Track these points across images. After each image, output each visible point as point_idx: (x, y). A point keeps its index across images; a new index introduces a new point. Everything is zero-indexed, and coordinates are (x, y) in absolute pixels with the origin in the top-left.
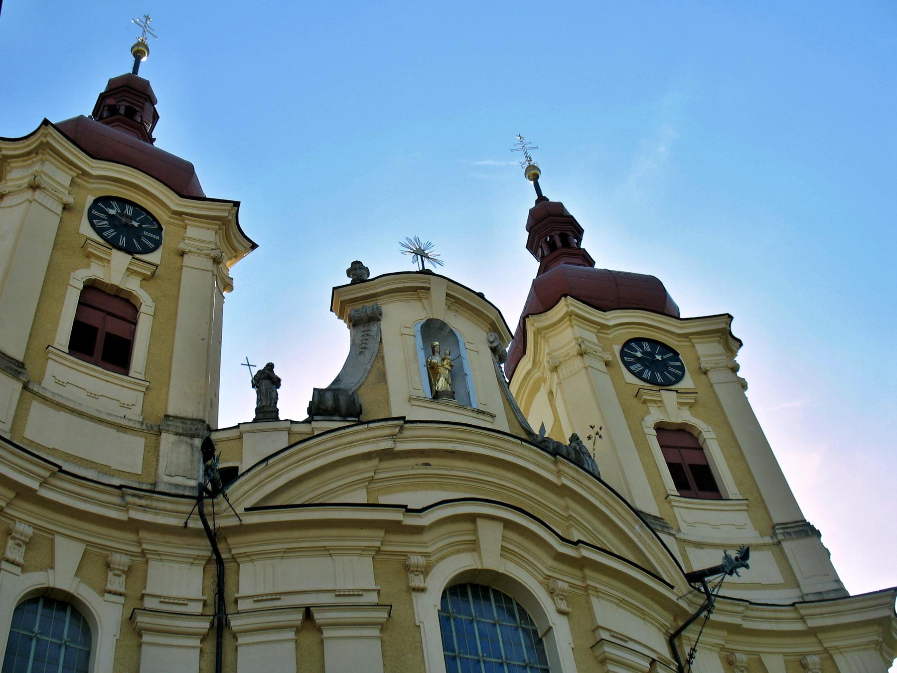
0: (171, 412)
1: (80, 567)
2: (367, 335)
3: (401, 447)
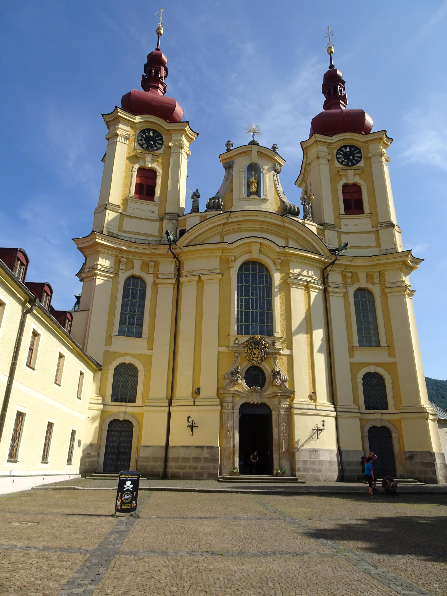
0: (167, 212)
3: (230, 220)
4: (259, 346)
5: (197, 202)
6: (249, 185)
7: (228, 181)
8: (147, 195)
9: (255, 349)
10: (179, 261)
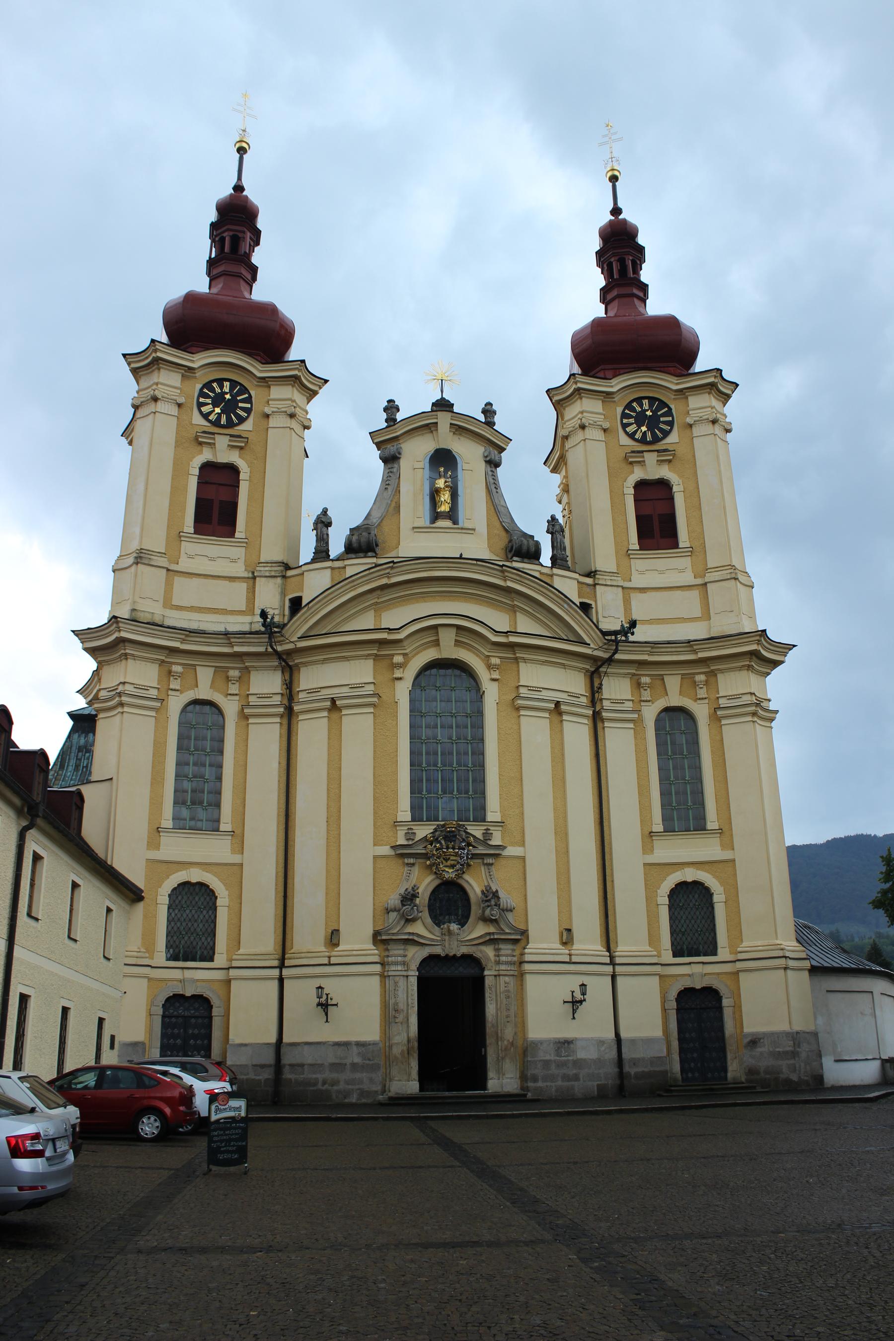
2: (391, 472)
4: (455, 843)
9: (447, 848)
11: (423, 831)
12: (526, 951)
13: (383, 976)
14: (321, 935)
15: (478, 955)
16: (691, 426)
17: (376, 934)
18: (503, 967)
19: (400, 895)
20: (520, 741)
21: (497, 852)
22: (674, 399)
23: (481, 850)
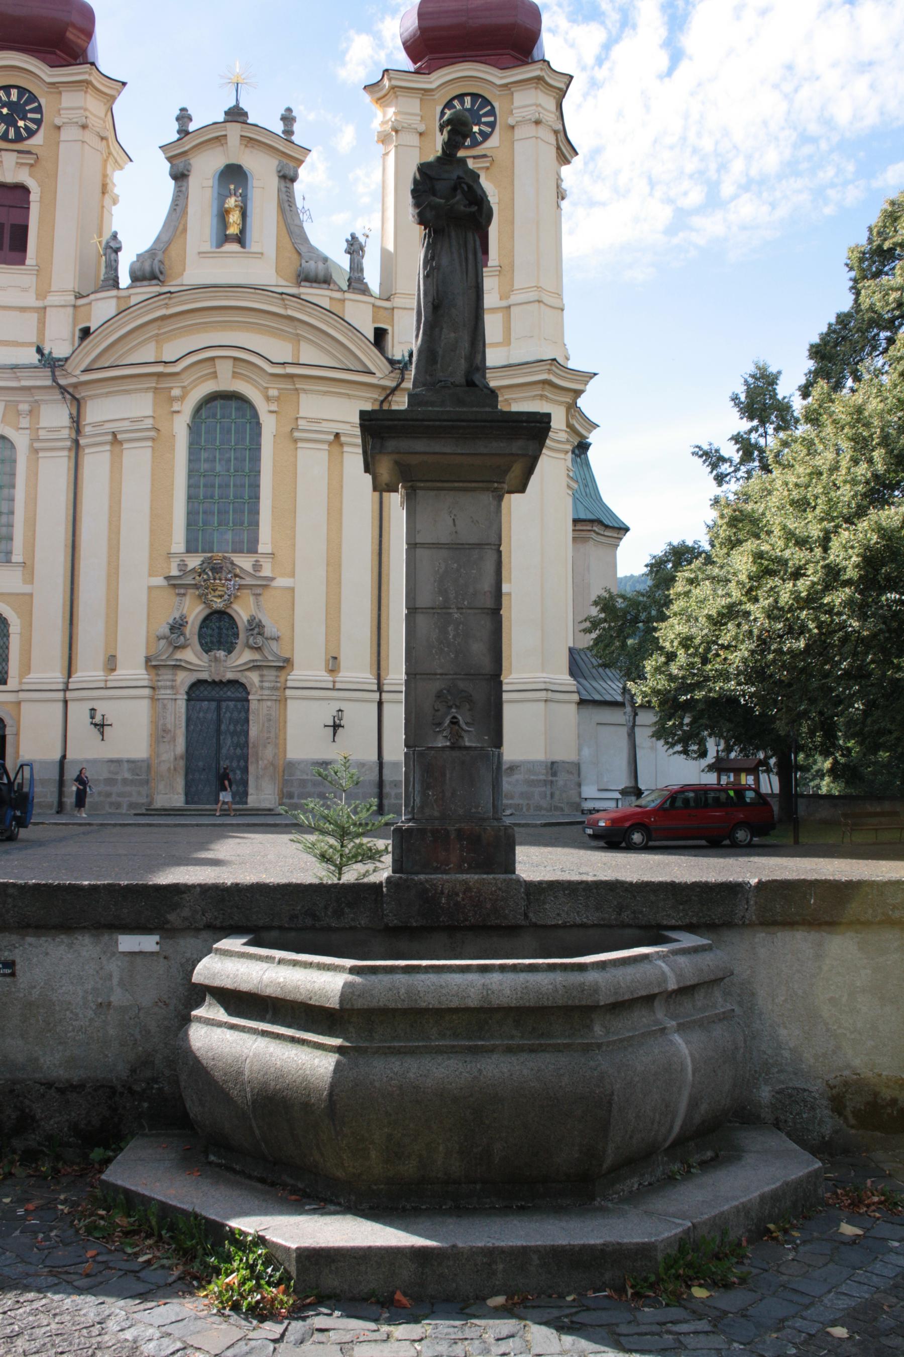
1: (4, 416)
5: (113, 263)
6: (223, 215)
7: (179, 209)
8: (13, 248)
9: (215, 579)
10: (78, 400)
11: (194, 562)
12: (289, 677)
13: (152, 698)
14: (101, 659)
15: (243, 680)
16: (513, 127)
17: (148, 660)
18: (266, 692)
19: (168, 623)
20: (296, 473)
21: (264, 583)
22: (500, 96)
23: (248, 581)
